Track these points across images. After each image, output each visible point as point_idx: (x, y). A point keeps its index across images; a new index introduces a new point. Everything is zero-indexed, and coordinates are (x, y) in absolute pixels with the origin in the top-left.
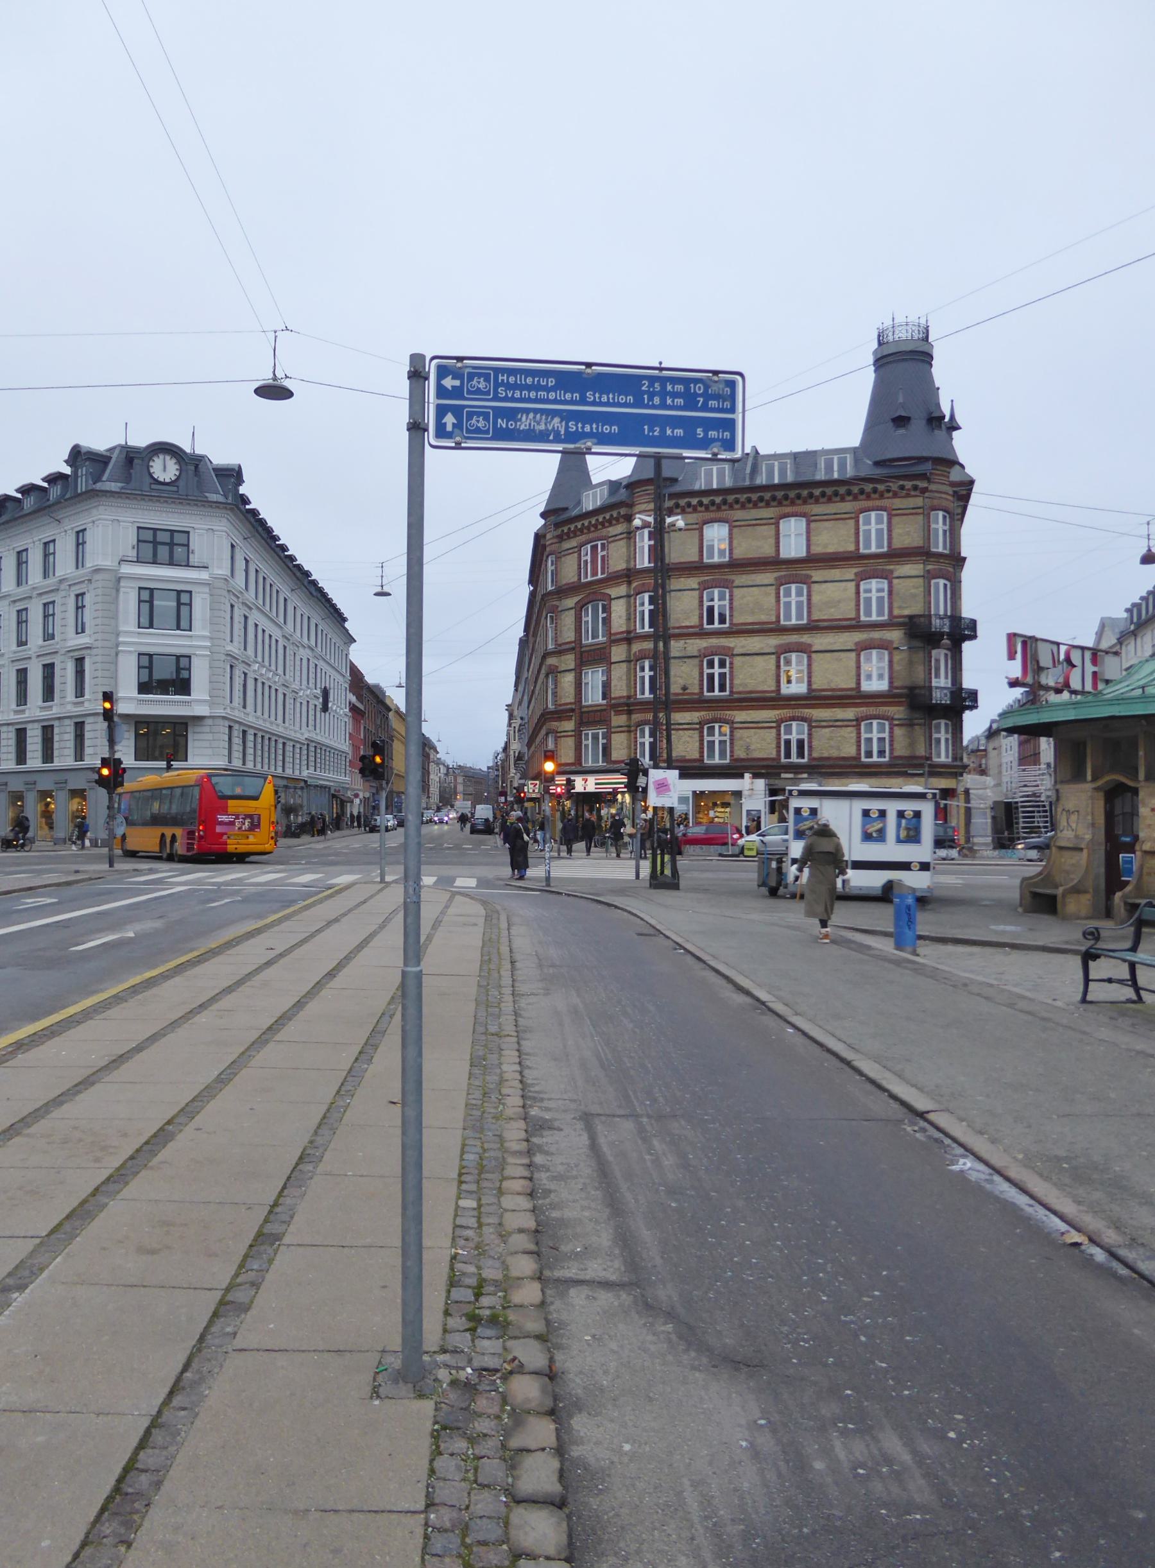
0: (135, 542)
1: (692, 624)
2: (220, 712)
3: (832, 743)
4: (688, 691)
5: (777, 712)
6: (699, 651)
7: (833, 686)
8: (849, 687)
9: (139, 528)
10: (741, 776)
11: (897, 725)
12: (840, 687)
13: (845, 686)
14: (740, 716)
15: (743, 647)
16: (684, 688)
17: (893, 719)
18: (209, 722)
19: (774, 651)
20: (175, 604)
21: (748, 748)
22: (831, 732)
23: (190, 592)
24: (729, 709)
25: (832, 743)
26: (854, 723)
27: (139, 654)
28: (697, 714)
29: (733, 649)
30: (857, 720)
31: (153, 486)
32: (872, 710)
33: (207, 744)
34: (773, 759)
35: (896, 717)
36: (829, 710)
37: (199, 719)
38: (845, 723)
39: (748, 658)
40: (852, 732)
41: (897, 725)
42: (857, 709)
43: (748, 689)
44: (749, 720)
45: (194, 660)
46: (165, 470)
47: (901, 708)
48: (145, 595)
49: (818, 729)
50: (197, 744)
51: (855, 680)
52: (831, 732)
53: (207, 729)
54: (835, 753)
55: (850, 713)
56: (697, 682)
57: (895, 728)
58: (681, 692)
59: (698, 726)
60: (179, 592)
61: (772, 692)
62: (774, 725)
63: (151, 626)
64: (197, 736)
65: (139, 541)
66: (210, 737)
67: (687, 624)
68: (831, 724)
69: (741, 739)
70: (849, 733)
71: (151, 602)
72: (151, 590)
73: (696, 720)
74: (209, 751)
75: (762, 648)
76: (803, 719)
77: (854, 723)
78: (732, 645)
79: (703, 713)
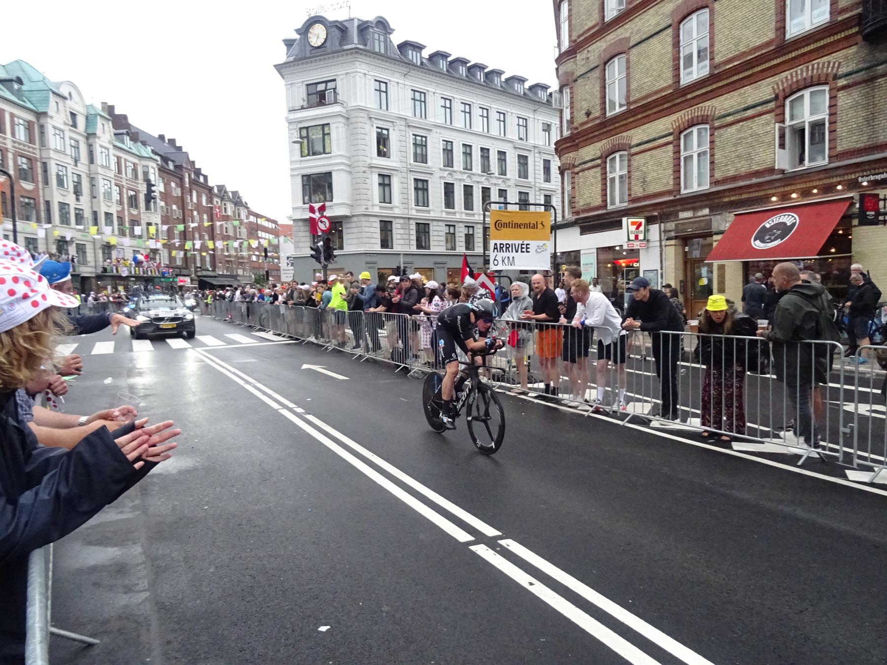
0: (305, 96)
1: (594, 23)
2: (361, 210)
3: (741, 150)
4: (591, 117)
5: (674, 117)
6: (600, 55)
7: (742, 48)
8: (766, 39)
9: (307, 85)
10: (618, 225)
11: (844, 88)
12: (752, 46)
13: (759, 43)
14: (638, 135)
15: (639, 31)
16: (588, 114)
17: (836, 77)
18: (355, 219)
19: (670, 22)
20: (321, 136)
21: (644, 182)
22: (739, 131)
23: (328, 124)
24: (627, 127)
25: (741, 150)
26: (772, 105)
27: (303, 176)
28: (599, 145)
29: (628, 39)
30: (776, 98)
31: (313, 52)
32: (800, 73)
33: (354, 236)
34: (669, 193)
35: (843, 70)
36: (735, 93)
37: (346, 217)
38: (759, 109)
39: (643, 45)
40: (768, 124)
41: (844, 88)
42: (776, 78)
43: (644, 94)
44: (645, 139)
45: (334, 175)
46: (318, 35)
47: (853, 50)
48: (304, 133)
49: (722, 131)
50: (349, 236)
51: (773, 25)
52: (739, 131)
53: (353, 225)
54: (743, 167)
55: (764, 90)
56: (598, 101)
57: (840, 94)
58: (586, 119)
59: (599, 161)
60: (323, 125)
61: (669, 87)
62: (670, 138)
63: (308, 155)
64: (349, 231)
65: (308, 95)
66: (356, 230)
67: (590, 24)
68: (738, 117)
69: (638, 168)
70: (767, 126)
71: (307, 137)
72: (307, 128)
73: (598, 154)
74: (356, 241)
75: (658, 24)
76: (704, 120)
77: (772, 105)
78: (627, 35)
79: (604, 141)
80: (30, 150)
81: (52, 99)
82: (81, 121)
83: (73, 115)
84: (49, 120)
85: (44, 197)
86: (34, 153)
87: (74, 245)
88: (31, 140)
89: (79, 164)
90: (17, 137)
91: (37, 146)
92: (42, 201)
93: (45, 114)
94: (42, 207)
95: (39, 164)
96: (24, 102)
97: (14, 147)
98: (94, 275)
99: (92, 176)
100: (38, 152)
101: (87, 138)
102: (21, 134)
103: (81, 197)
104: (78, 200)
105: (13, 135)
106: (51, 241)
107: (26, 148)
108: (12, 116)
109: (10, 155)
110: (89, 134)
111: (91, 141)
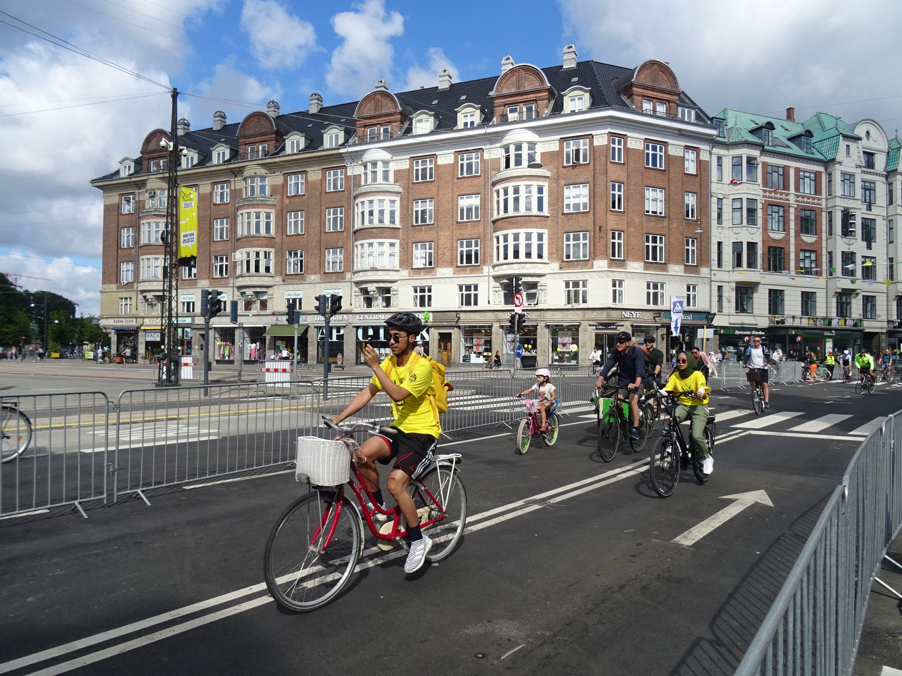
80: (816, 201)
81: (843, 144)
82: (880, 162)
83: (869, 156)
84: (837, 166)
85: (826, 248)
86: (819, 204)
87: (860, 297)
88: (818, 191)
89: (873, 208)
90: (802, 190)
91: (824, 196)
92: (824, 252)
93: (833, 160)
94: (825, 259)
95: (824, 215)
96: (813, 154)
97: (796, 201)
98: (884, 331)
99: (890, 218)
100: (824, 201)
101: (887, 177)
102: (807, 188)
103: (873, 244)
104: (869, 247)
105: (797, 189)
106: (831, 293)
107: (811, 200)
108: (797, 170)
109: (792, 210)
110: (889, 173)
111: (890, 180)
